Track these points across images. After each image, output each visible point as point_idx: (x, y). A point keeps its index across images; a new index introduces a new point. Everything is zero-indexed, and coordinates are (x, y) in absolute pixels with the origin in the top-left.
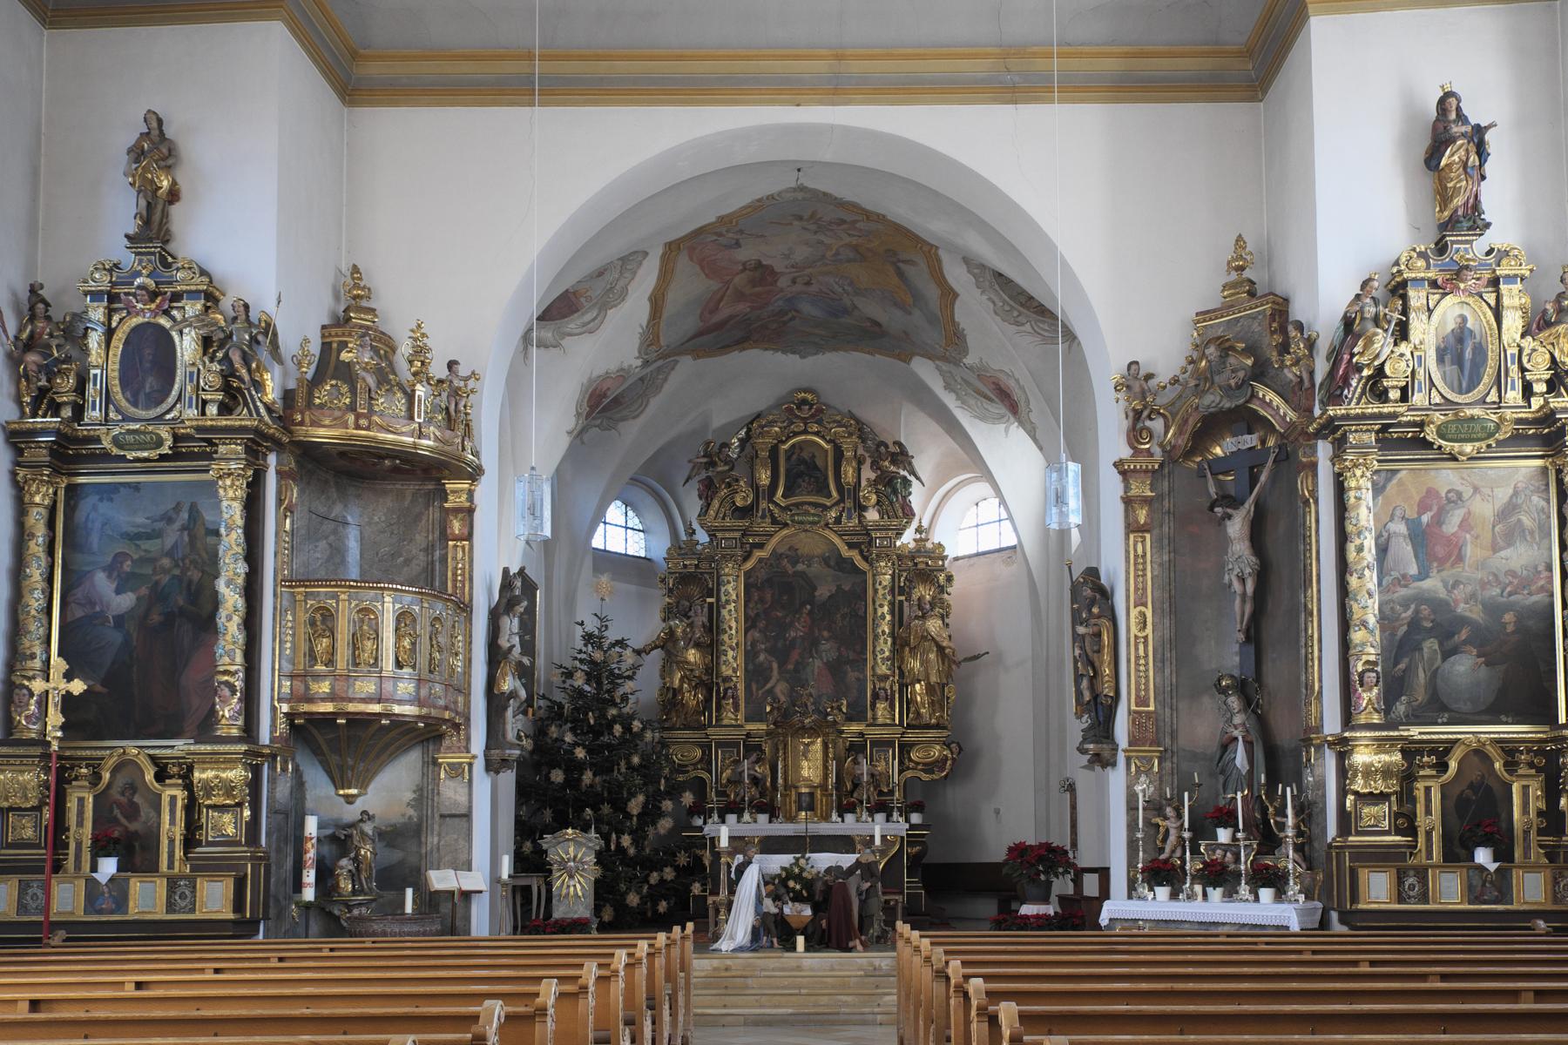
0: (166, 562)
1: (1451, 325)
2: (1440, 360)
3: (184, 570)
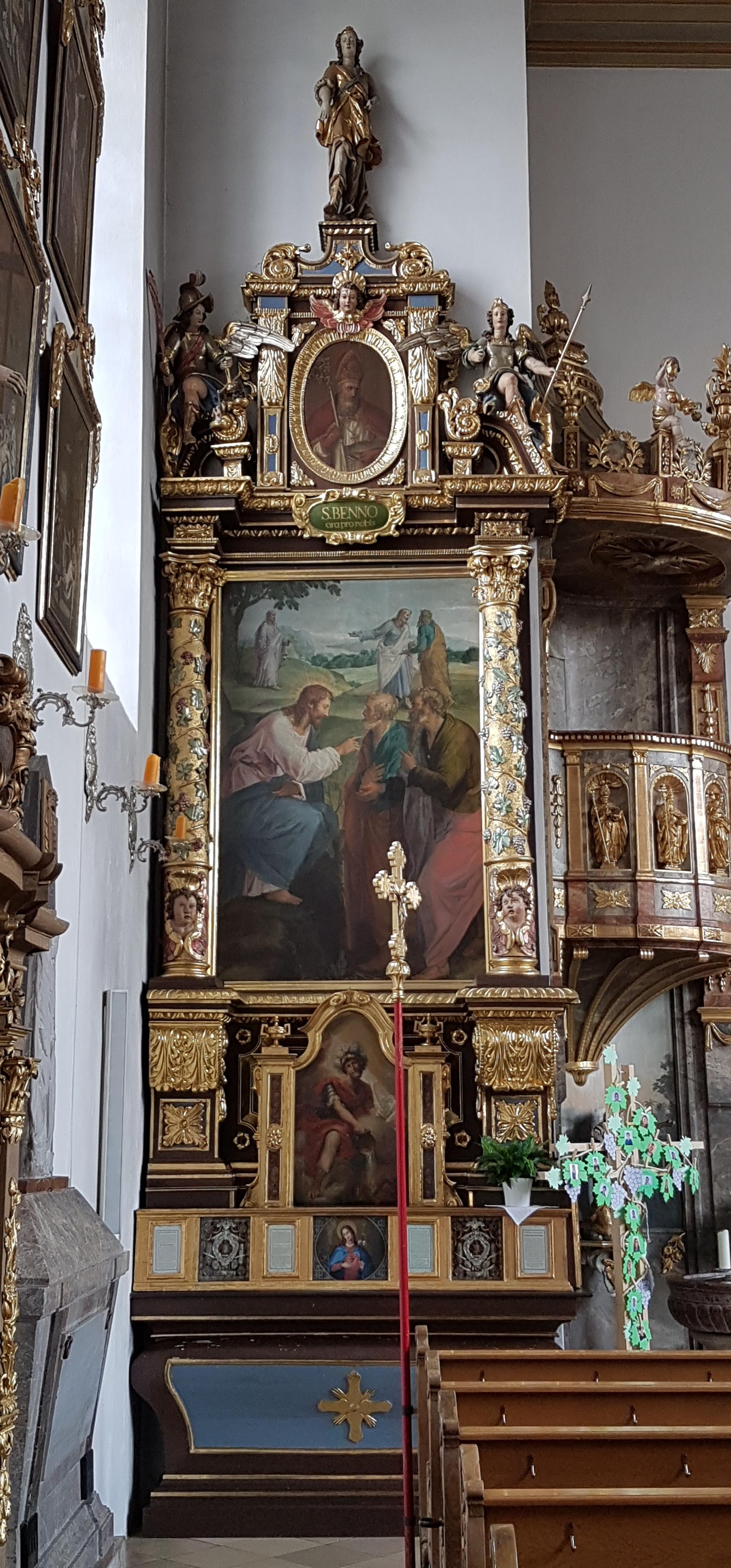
0: (385, 701)
3: (415, 715)
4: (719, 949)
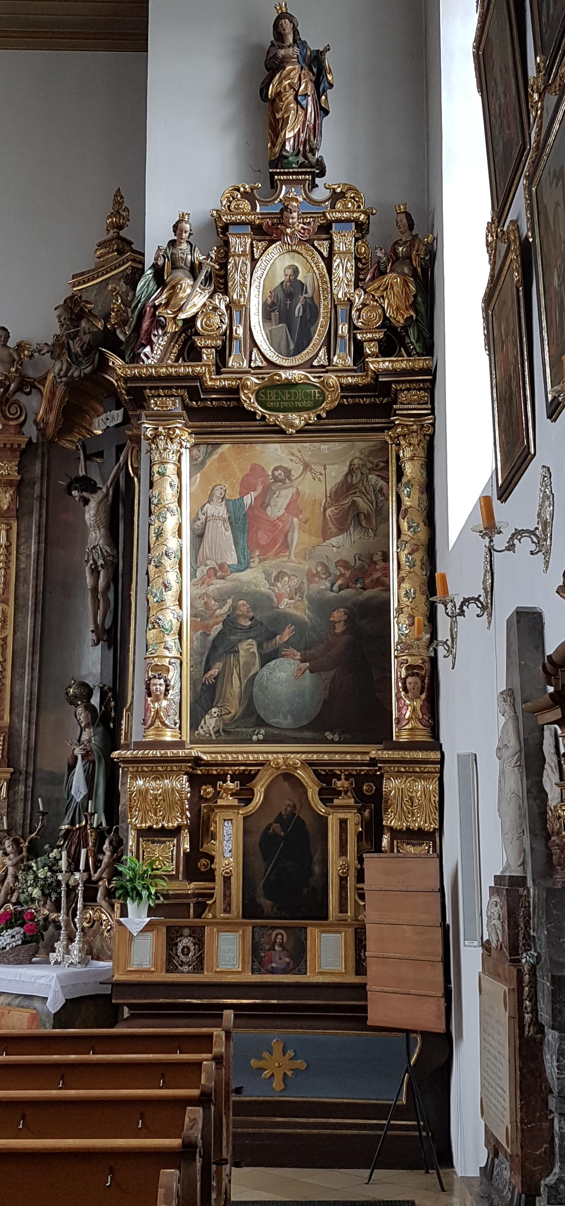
1: (280, 278)
2: (267, 316)
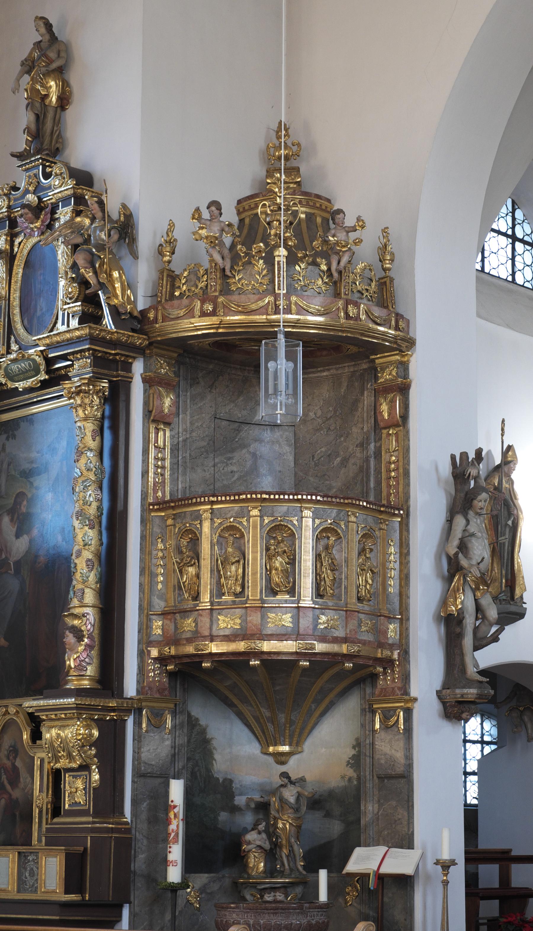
4: (272, 655)
